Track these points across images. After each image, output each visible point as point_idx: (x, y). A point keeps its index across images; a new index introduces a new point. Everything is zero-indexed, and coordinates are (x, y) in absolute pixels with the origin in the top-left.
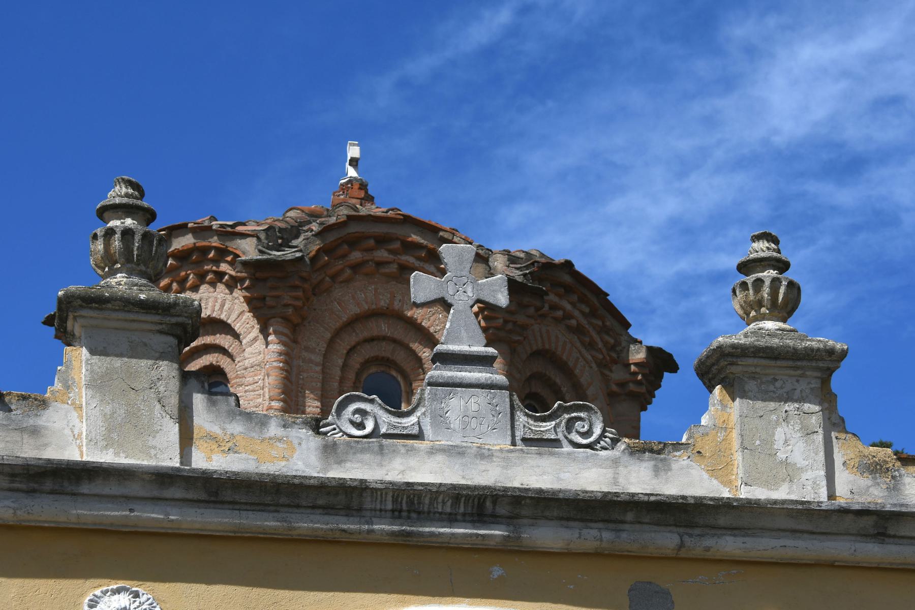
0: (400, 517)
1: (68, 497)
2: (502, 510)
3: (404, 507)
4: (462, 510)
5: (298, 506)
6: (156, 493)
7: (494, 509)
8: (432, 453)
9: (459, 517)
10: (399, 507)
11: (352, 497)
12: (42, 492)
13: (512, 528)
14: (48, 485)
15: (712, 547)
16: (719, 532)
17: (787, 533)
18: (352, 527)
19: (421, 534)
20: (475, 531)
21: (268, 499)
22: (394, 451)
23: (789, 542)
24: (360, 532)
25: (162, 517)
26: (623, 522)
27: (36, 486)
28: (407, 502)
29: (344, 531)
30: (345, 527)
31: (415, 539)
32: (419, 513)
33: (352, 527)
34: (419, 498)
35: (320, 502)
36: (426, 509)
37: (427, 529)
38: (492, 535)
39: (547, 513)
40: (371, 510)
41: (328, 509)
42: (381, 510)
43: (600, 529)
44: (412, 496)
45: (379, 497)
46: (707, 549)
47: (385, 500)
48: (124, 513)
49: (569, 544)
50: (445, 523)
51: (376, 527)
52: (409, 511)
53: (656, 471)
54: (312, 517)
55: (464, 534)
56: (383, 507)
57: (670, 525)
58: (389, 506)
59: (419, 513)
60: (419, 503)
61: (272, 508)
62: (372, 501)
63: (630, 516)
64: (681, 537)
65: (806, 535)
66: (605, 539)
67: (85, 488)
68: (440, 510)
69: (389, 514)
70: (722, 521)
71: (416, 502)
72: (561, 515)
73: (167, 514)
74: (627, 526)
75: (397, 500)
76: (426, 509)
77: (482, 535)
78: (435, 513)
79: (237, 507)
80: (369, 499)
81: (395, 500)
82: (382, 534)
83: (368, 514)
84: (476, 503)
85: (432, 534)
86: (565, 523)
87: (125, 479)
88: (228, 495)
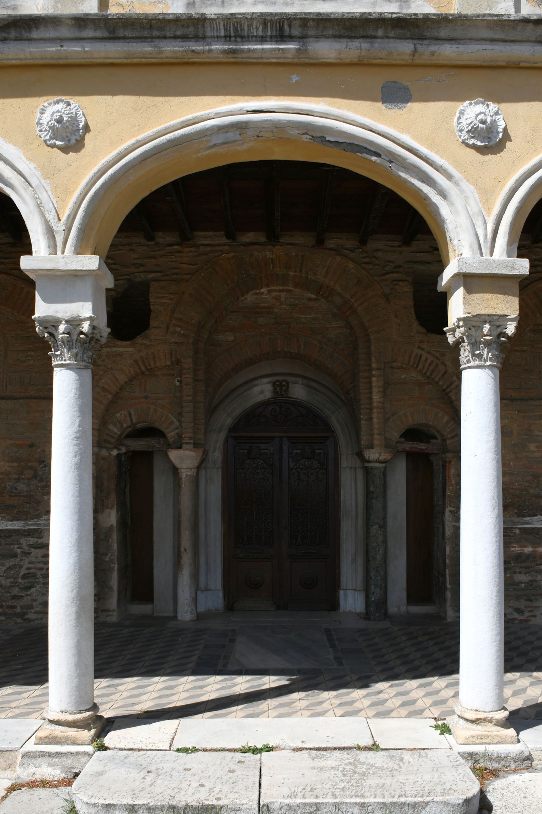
0: (230, 41)
1: (26, 42)
2: (296, 32)
3: (232, 34)
4: (269, 33)
5: (165, 38)
6: (77, 34)
7: (290, 31)
8: (255, 4)
9: (268, 39)
10: (229, 33)
11: (198, 28)
12: (11, 40)
13: (301, 43)
14: (13, 34)
15: (435, 52)
16: (442, 42)
17: (487, 42)
18: (198, 48)
19: (242, 51)
20: (277, 46)
21: (146, 33)
22: (231, 4)
23: (489, 47)
24: (203, 52)
25: (80, 49)
26: (375, 37)
27: (6, 35)
28: (233, 30)
29: (193, 51)
30: (193, 48)
31: (240, 56)
32: (242, 37)
33: (198, 48)
34: (241, 25)
35: (178, 33)
36: (246, 34)
37: (246, 47)
38: (288, 49)
39: (325, 33)
40: (212, 37)
41: (184, 38)
42: (218, 37)
43: (360, 43)
44: (236, 24)
45: (215, 27)
46: (433, 54)
47: (220, 29)
48: (57, 48)
49: (340, 54)
50: (258, 43)
51: (213, 47)
52: (235, 37)
53: (401, 7)
54: (173, 43)
55: (270, 49)
56: (218, 34)
57: (408, 39)
58: (222, 33)
59: (242, 37)
60: (241, 30)
61: (149, 40)
62: (211, 30)
63: (380, 33)
64: (415, 45)
65: (500, 43)
66: (363, 48)
67: (35, 34)
68: (255, 34)
69: (223, 39)
70: (443, 33)
71: (239, 29)
72: (334, 34)
73: (83, 48)
74: (379, 40)
75: (227, 29)
76: (246, 34)
77: (282, 49)
78: (252, 36)
79: (128, 41)
80: (209, 29)
81: (226, 29)
82: (218, 53)
83: (210, 40)
84: (278, 27)
85: (249, 50)
86: (337, 39)
87: (57, 25)
88: (121, 33)
